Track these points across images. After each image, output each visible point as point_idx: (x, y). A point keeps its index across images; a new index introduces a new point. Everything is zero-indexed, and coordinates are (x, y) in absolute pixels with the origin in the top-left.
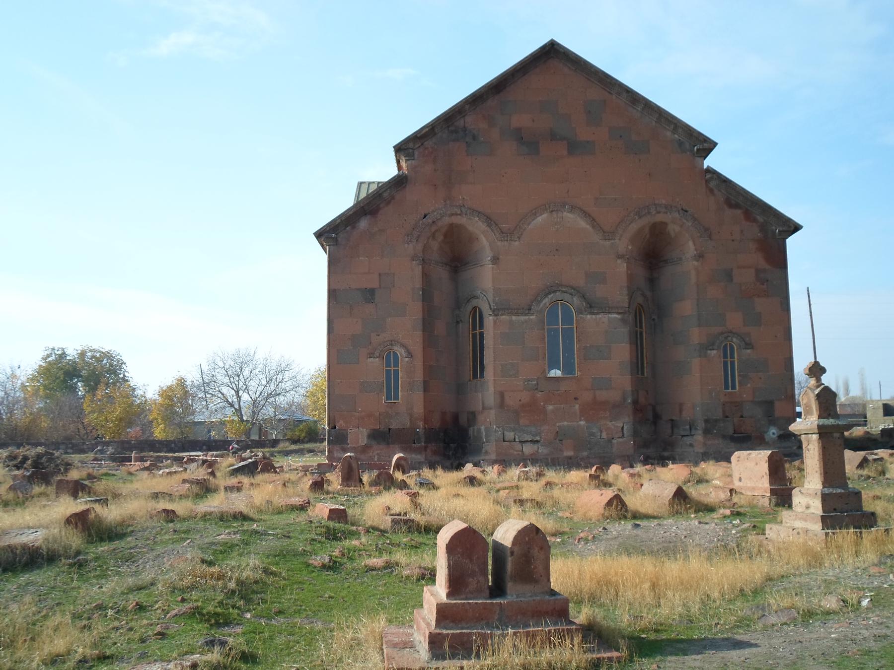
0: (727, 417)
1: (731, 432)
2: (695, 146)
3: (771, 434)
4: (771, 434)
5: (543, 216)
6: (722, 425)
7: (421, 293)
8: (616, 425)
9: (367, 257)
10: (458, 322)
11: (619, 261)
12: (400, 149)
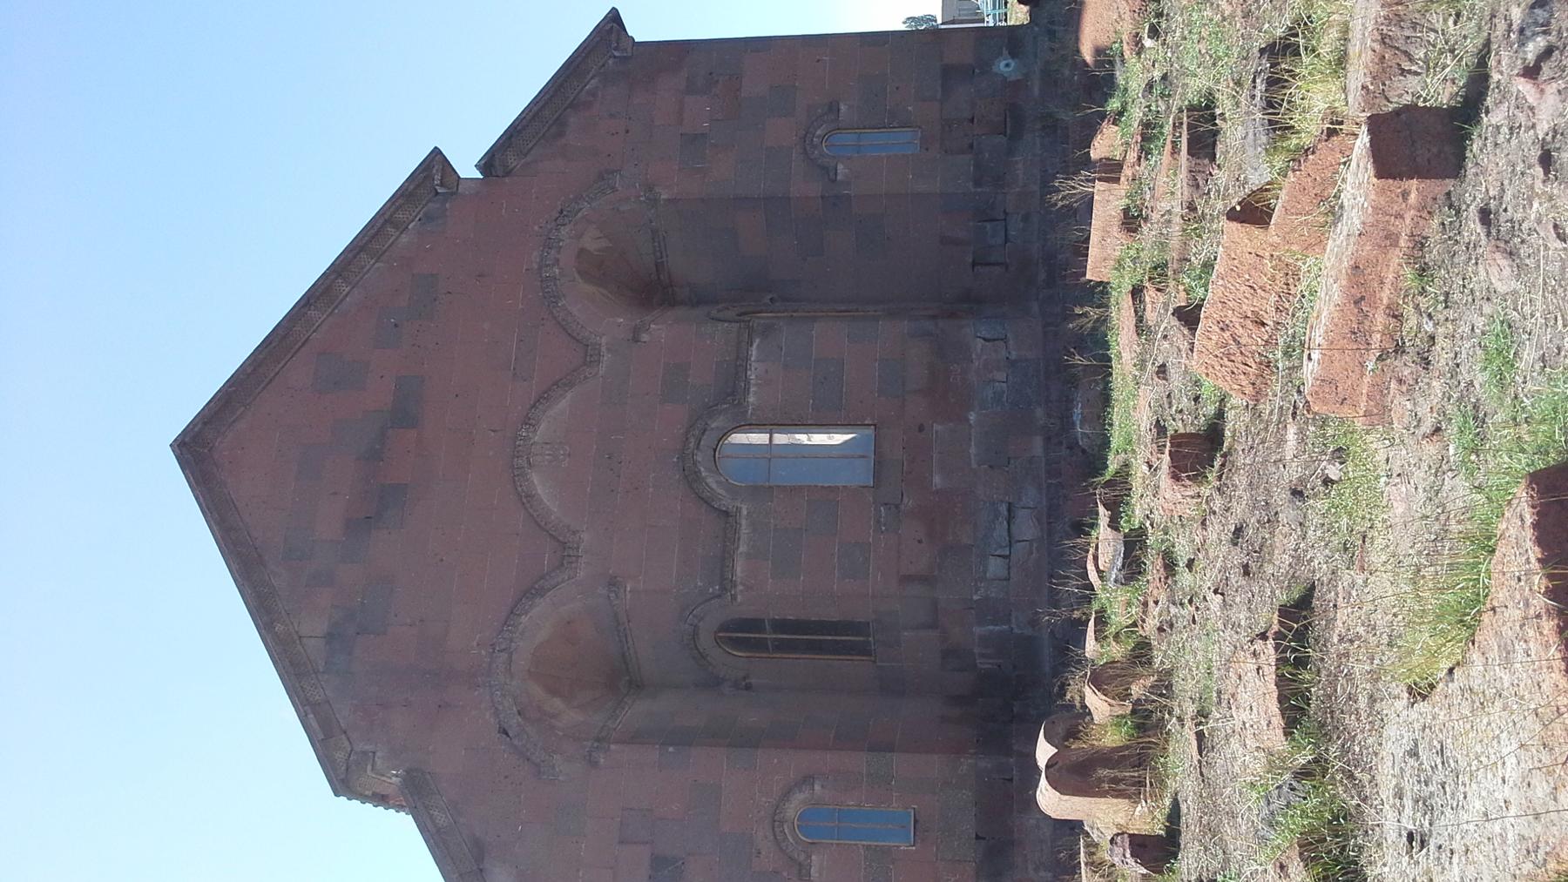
0: (971, 146)
1: (1001, 139)
2: (437, 193)
4: (1007, 69)
5: (536, 482)
7: (671, 749)
8: (979, 351)
9: (578, 870)
10: (748, 687)
11: (645, 337)
12: (344, 781)
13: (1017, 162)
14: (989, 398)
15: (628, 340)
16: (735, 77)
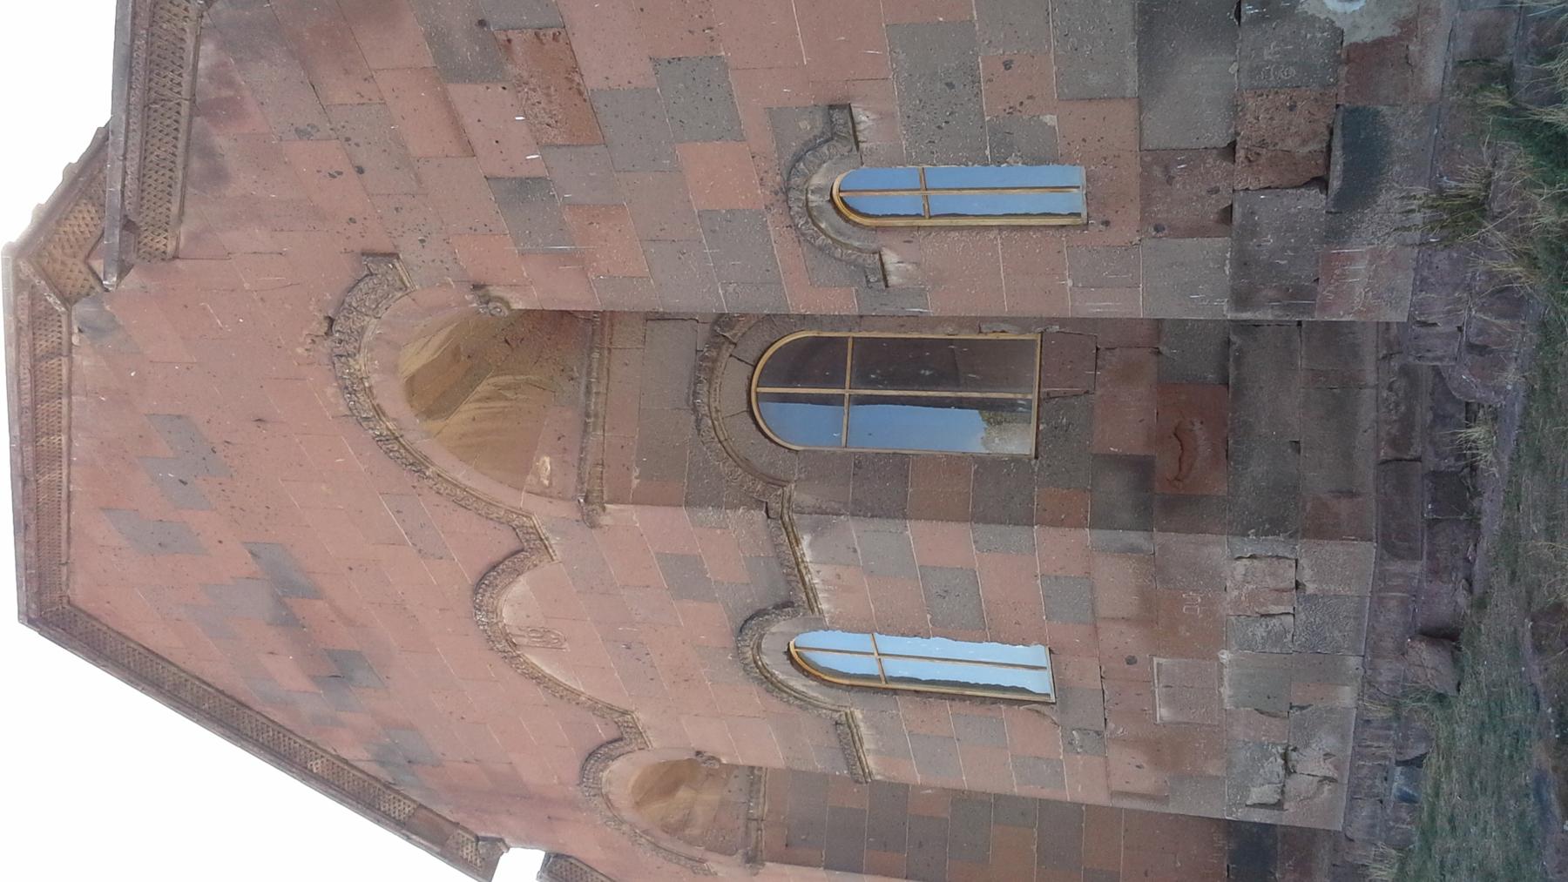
0: (1227, 214)
1: (1314, 200)
5: (534, 661)
6: (1270, 240)
14: (1258, 639)
15: (577, 521)
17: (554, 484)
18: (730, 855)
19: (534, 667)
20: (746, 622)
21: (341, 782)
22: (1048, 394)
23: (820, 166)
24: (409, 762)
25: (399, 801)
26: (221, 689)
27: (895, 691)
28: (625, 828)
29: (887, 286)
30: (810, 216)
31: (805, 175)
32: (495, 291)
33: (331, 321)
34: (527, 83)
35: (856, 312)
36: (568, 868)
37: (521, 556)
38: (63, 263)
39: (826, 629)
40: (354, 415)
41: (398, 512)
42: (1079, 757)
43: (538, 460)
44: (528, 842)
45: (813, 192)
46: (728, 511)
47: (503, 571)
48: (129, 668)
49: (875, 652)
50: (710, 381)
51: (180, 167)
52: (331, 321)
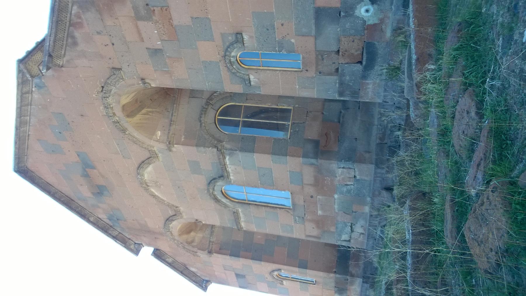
0: (337, 69)
1: (359, 67)
3: (369, 14)
5: (153, 191)
6: (348, 78)
11: (174, 149)
12: (136, 252)
13: (368, 84)
16: (165, 8)
17: (161, 139)
18: (204, 251)
19: (153, 192)
20: (211, 181)
21: (98, 224)
22: (294, 122)
23: (234, 50)
24: (118, 220)
25: (114, 231)
26: (67, 195)
27: (250, 204)
28: (176, 242)
29: (250, 85)
30: (231, 64)
31: (230, 52)
32: (147, 81)
33: (103, 87)
34: (158, 22)
35: (242, 92)
36: (160, 253)
37: (151, 159)
38: (32, 66)
39: (232, 184)
40: (107, 115)
41: (118, 144)
42: (298, 224)
43: (157, 132)
44: (149, 245)
45: (232, 57)
46: (207, 148)
47: (146, 163)
48: (41, 187)
49: (245, 192)
50: (205, 114)
51: (65, 40)
52: (103, 87)
